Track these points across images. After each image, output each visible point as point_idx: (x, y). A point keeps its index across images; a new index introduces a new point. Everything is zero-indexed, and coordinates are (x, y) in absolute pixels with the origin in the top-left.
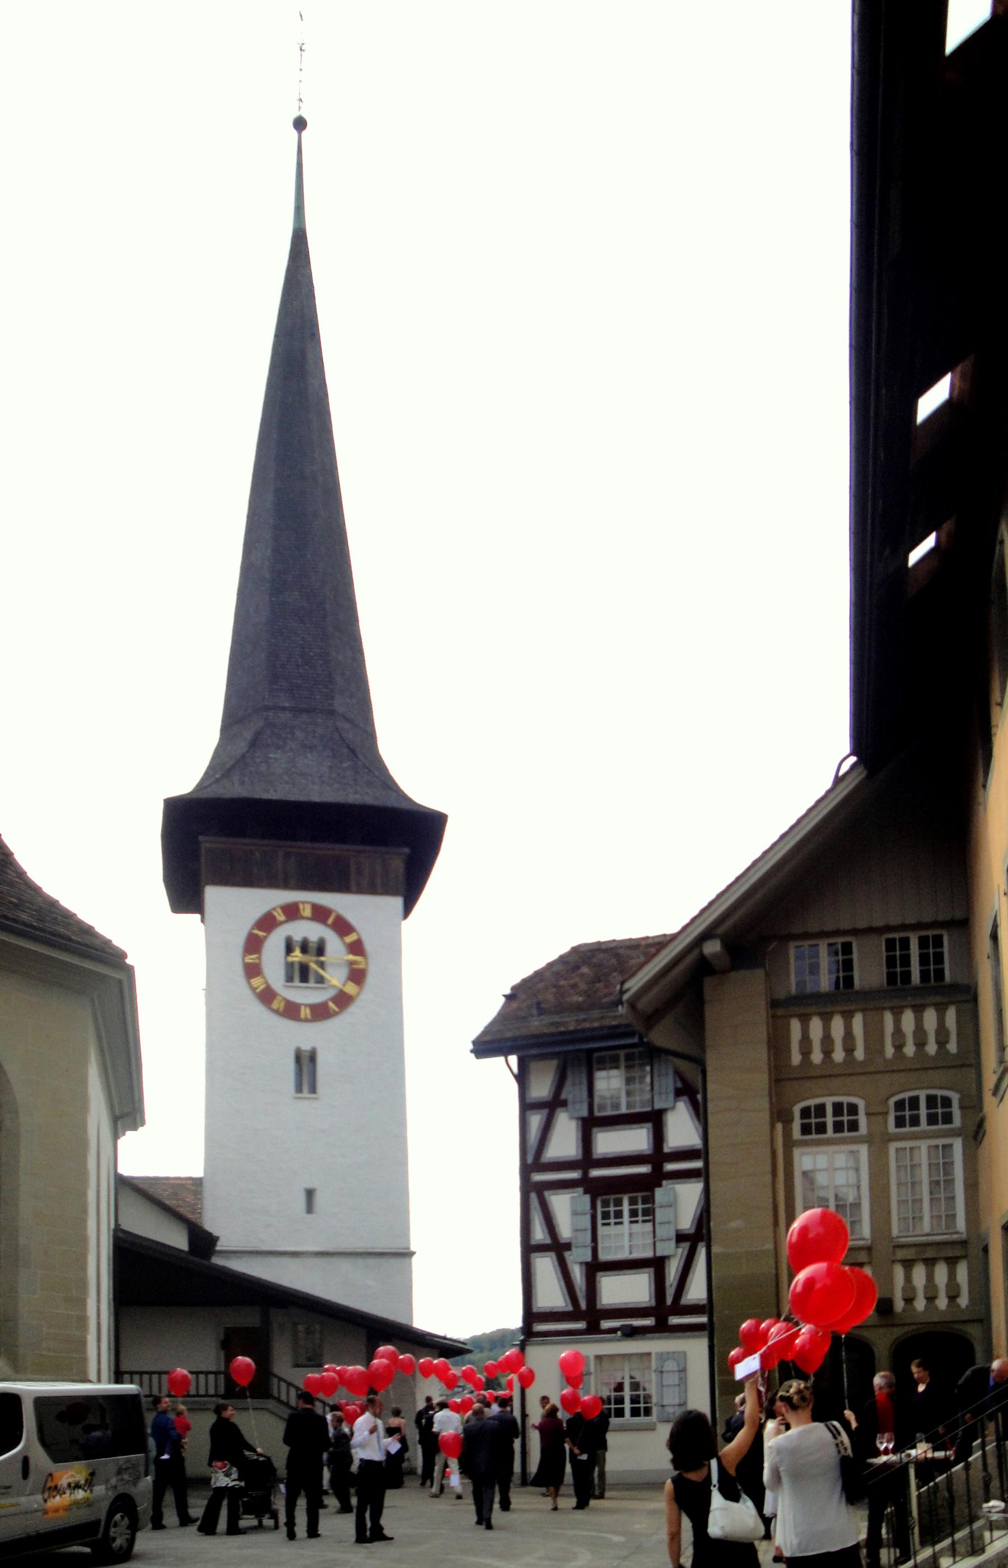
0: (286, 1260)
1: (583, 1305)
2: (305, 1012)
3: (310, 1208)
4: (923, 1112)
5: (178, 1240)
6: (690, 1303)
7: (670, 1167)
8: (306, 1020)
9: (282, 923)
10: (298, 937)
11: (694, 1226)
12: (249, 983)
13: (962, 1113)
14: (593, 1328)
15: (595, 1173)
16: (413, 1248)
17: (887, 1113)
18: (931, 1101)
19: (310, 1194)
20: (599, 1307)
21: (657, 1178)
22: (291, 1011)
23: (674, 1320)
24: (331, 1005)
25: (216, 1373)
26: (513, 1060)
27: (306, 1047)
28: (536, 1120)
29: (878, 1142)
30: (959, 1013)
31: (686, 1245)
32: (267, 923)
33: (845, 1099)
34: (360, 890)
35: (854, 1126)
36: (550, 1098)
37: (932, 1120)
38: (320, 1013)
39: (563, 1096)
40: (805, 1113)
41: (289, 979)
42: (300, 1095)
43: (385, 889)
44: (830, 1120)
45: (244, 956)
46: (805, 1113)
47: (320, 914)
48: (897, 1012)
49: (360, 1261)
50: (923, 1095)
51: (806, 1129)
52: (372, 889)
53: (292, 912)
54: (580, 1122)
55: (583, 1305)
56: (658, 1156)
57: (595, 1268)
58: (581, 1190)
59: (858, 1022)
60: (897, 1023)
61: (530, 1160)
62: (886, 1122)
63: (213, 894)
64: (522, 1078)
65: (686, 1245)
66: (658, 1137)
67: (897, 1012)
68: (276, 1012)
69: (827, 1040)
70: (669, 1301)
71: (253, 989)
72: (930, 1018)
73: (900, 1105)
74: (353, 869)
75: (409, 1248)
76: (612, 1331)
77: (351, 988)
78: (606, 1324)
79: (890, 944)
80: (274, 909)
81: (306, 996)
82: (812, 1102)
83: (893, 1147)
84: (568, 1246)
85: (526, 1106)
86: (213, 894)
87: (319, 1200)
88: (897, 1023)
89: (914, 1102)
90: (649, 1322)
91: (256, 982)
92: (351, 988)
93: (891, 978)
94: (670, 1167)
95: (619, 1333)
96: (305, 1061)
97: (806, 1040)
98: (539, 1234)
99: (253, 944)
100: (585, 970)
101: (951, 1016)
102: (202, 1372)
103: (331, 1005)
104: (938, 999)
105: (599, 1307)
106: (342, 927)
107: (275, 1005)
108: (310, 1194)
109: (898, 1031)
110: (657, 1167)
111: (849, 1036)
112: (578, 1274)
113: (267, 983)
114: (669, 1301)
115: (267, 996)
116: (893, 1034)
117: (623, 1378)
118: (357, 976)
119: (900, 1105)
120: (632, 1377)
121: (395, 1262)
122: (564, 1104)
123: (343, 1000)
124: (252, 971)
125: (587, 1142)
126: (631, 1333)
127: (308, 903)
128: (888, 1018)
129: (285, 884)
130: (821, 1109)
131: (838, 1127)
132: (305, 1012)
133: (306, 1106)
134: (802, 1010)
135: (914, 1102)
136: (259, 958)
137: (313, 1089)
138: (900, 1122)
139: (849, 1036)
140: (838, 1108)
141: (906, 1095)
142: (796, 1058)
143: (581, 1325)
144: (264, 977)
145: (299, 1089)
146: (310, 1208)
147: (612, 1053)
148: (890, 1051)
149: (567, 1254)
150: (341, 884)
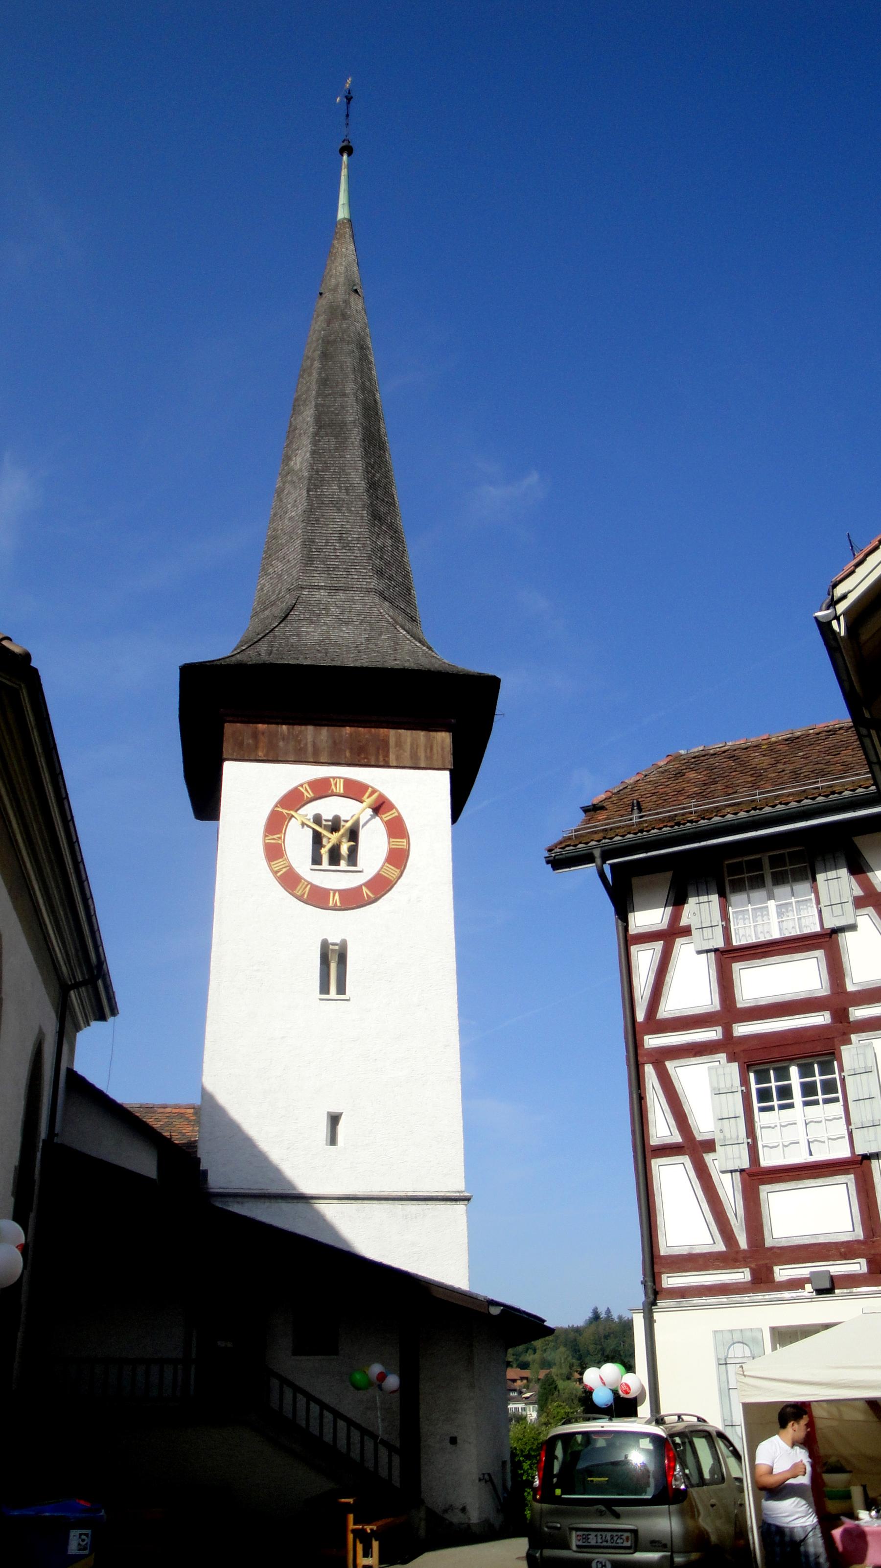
1: (743, 1242)
8: (335, 908)
12: (270, 866)
19: (334, 1120)
20: (769, 1243)
24: (365, 890)
39: (684, 922)
41: (316, 860)
45: (265, 836)
47: (354, 791)
53: (321, 789)
55: (743, 1242)
68: (300, 898)
71: (275, 873)
76: (796, 1284)
78: (782, 1273)
80: (302, 785)
84: (709, 1146)
91: (278, 864)
95: (808, 1287)
103: (365, 890)
105: (769, 1243)
106: (380, 807)
108: (334, 1120)
124: (274, 852)
127: (340, 778)
137: (341, 989)
145: (324, 988)
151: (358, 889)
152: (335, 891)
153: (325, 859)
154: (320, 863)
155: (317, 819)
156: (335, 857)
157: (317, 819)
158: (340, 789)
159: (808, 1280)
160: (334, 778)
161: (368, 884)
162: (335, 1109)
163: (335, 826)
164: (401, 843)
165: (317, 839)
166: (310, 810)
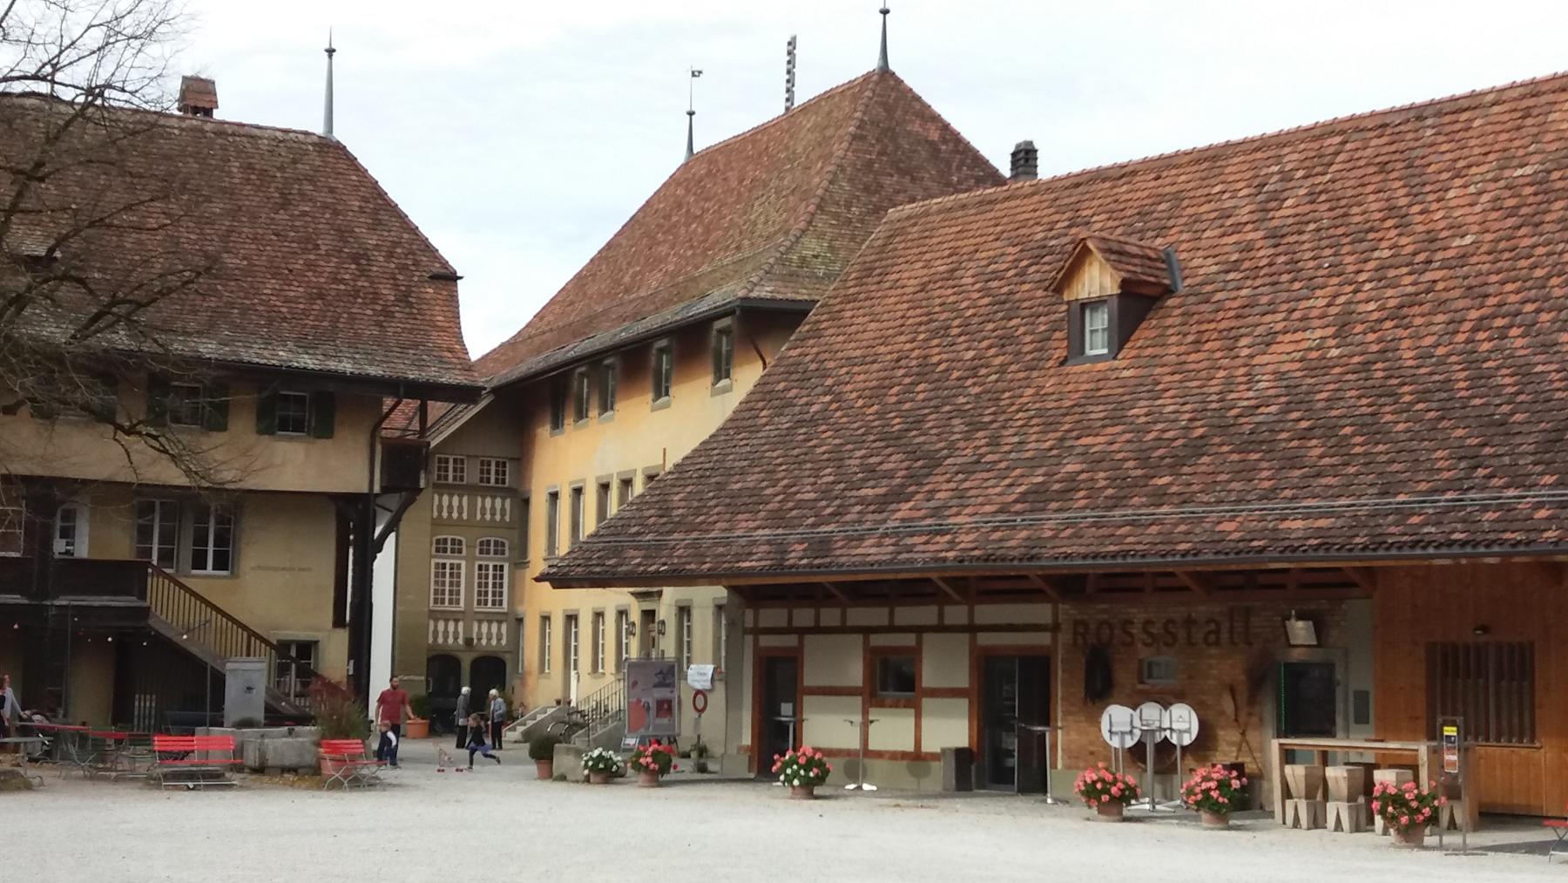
4: (492, 548)
18: (496, 543)
29: (470, 560)
35: (460, 551)
37: (496, 553)
40: (438, 542)
44: (449, 546)
48: (484, 498)
50: (492, 539)
59: (465, 499)
72: (498, 502)
73: (482, 543)
89: (489, 541)
104: (502, 494)
109: (483, 508)
111: (460, 507)
128: (479, 499)
130: (445, 540)
138: (481, 552)
139: (460, 507)
140: (453, 541)
141: (484, 539)
148: (479, 517)
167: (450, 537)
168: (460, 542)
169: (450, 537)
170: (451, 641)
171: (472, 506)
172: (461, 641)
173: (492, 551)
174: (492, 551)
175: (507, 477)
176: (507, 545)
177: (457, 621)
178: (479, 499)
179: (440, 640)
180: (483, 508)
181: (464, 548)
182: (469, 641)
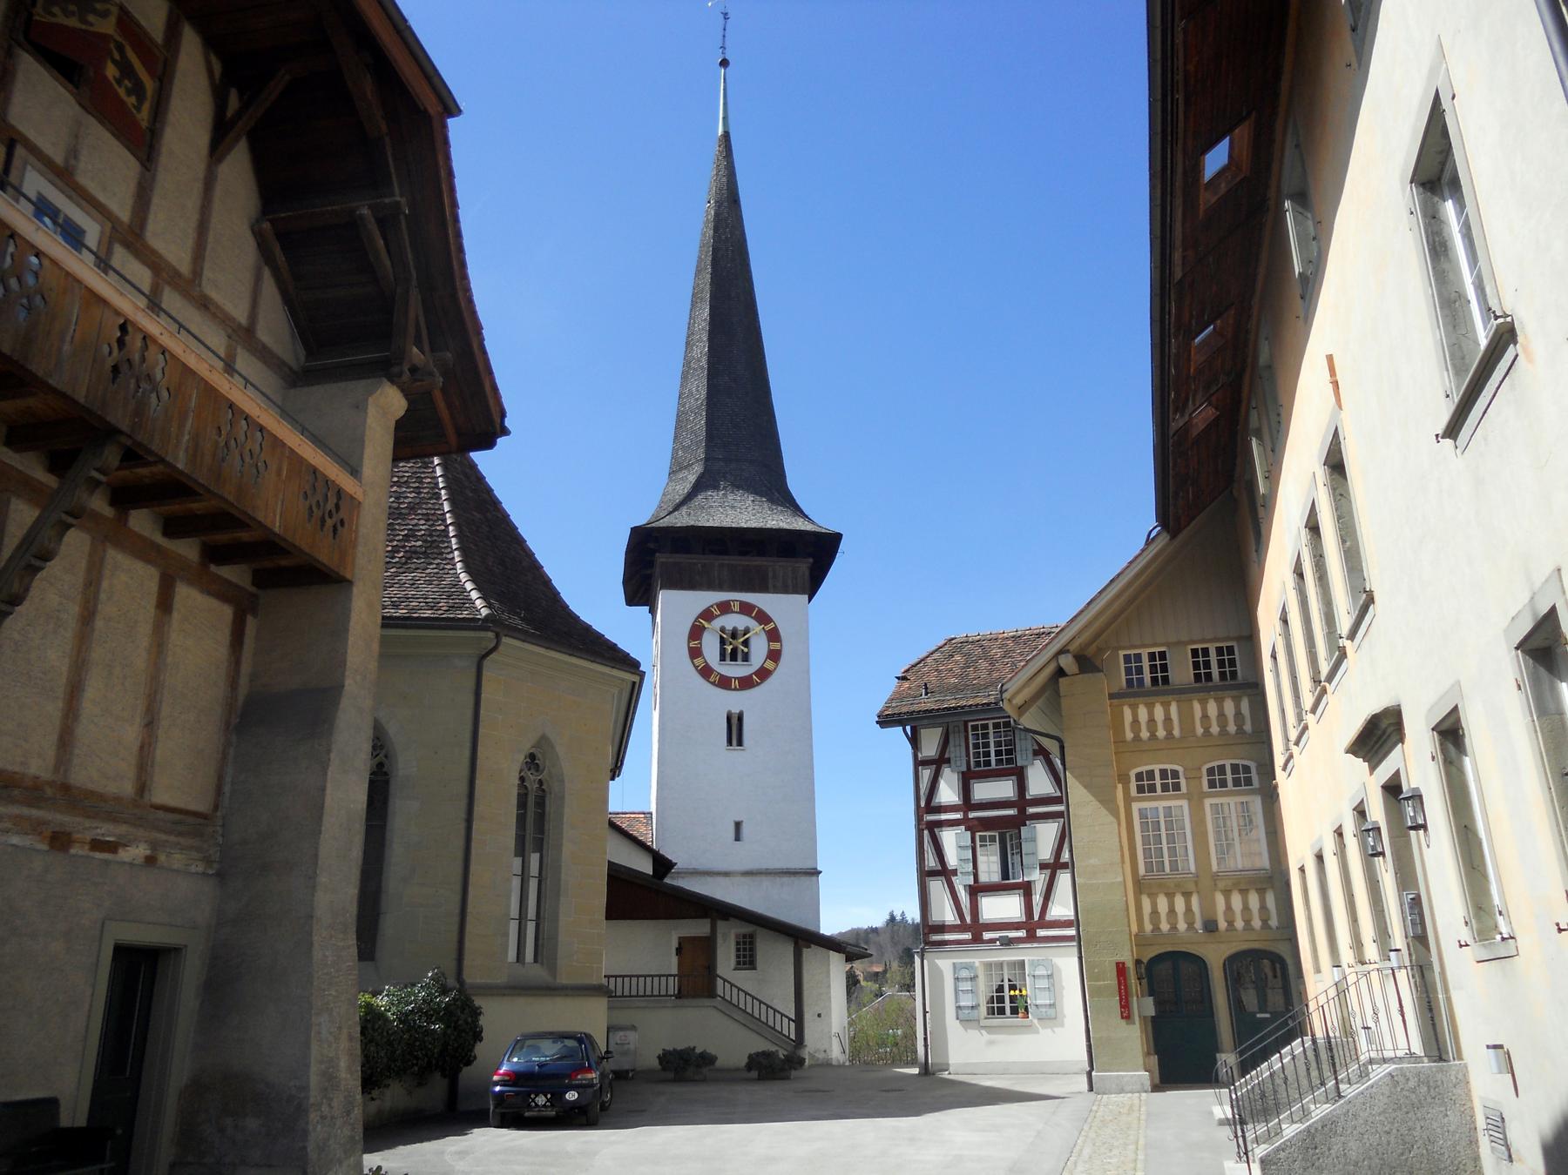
0: (721, 880)
2: (735, 684)
3: (738, 838)
4: (1229, 777)
5: (645, 866)
6: (1053, 919)
7: (1031, 810)
8: (735, 689)
9: (717, 616)
10: (729, 627)
11: (1053, 857)
12: (693, 663)
13: (1259, 778)
14: (977, 939)
15: (972, 815)
16: (819, 869)
17: (1201, 777)
18: (1235, 768)
19: (738, 825)
20: (981, 922)
21: (1021, 820)
22: (724, 683)
23: (1041, 933)
25: (674, 976)
26: (908, 728)
27: (735, 710)
28: (926, 774)
29: (1196, 800)
30: (1251, 702)
31: (1048, 872)
32: (707, 615)
33: (1168, 767)
34: (776, 591)
35: (1177, 787)
36: (937, 757)
37: (1237, 782)
38: (746, 683)
40: (1139, 777)
41: (723, 658)
42: (731, 748)
43: (796, 591)
44: (1158, 782)
45: (689, 642)
46: (1139, 777)
47: (746, 609)
48: (1203, 703)
49: (778, 880)
50: (1228, 763)
51: (1140, 789)
52: (785, 589)
53: (725, 608)
54: (960, 775)
56: (1022, 800)
57: (977, 890)
58: (963, 827)
59: (1174, 708)
60: (1204, 710)
61: (923, 804)
62: (1201, 783)
63: (664, 597)
64: (914, 741)
65: (1048, 872)
66: (1022, 787)
67: (1203, 703)
68: (713, 683)
69: (1152, 721)
70: (1036, 917)
71: (696, 667)
73: (1211, 771)
74: (770, 575)
75: (816, 869)
76: (992, 941)
77: (770, 665)
78: (987, 936)
79: (1195, 653)
80: (712, 606)
81: (735, 670)
82: (1144, 769)
83: (1208, 802)
84: (955, 872)
85: (919, 763)
86: (664, 597)
87: (745, 830)
88: (1204, 710)
89: (1222, 769)
90: (1022, 934)
91: (698, 661)
92: (770, 665)
93: (1197, 677)
94: (1031, 810)
95: (998, 943)
96: (735, 721)
97: (1136, 721)
98: (931, 862)
99: (696, 632)
100: (957, 657)
101: (1245, 705)
102: (663, 976)
104: (1235, 693)
106: (763, 618)
107: (712, 679)
108: (738, 825)
109: (1205, 717)
110: (1022, 811)
111: (1168, 719)
112: (963, 896)
113: (706, 662)
114: (1036, 917)
115: (706, 672)
116: (1201, 718)
117: (1002, 981)
118: (774, 656)
119: (1211, 771)
120: (1009, 980)
121: (805, 880)
122: (948, 761)
123: (764, 674)
124: (695, 653)
125: (966, 791)
126: (1008, 942)
128: (1197, 706)
129: (720, 587)
130: (1151, 774)
131: (1165, 788)
132: (735, 684)
133: (735, 754)
134: (1132, 700)
135: (1222, 769)
136: (700, 643)
137: (740, 743)
138: (1212, 784)
139: (1168, 719)
140: (1164, 773)
141: (1215, 764)
142: (1129, 735)
143: (968, 936)
144: (704, 658)
145: (730, 742)
146: (738, 838)
147: (983, 722)
148: (1200, 731)
149: (954, 879)
150: (763, 588)
151: (751, 676)
152: (735, 678)
153: (728, 658)
154: (724, 660)
155: (723, 630)
156: (734, 657)
157: (723, 630)
158: (737, 609)
159: (997, 939)
160: (733, 601)
161: (756, 673)
162: (737, 819)
163: (734, 634)
164: (775, 646)
165: (723, 641)
166: (718, 623)
167: (1157, 768)
168: (1175, 774)
169: (1157, 768)
170: (1182, 926)
171: (1187, 718)
172: (1198, 925)
173: (1230, 783)
174: (1230, 783)
175: (1237, 655)
176: (1254, 770)
177: (1187, 895)
178: (1197, 706)
179: (1165, 927)
180: (1205, 717)
181: (1183, 781)
182: (1210, 926)
